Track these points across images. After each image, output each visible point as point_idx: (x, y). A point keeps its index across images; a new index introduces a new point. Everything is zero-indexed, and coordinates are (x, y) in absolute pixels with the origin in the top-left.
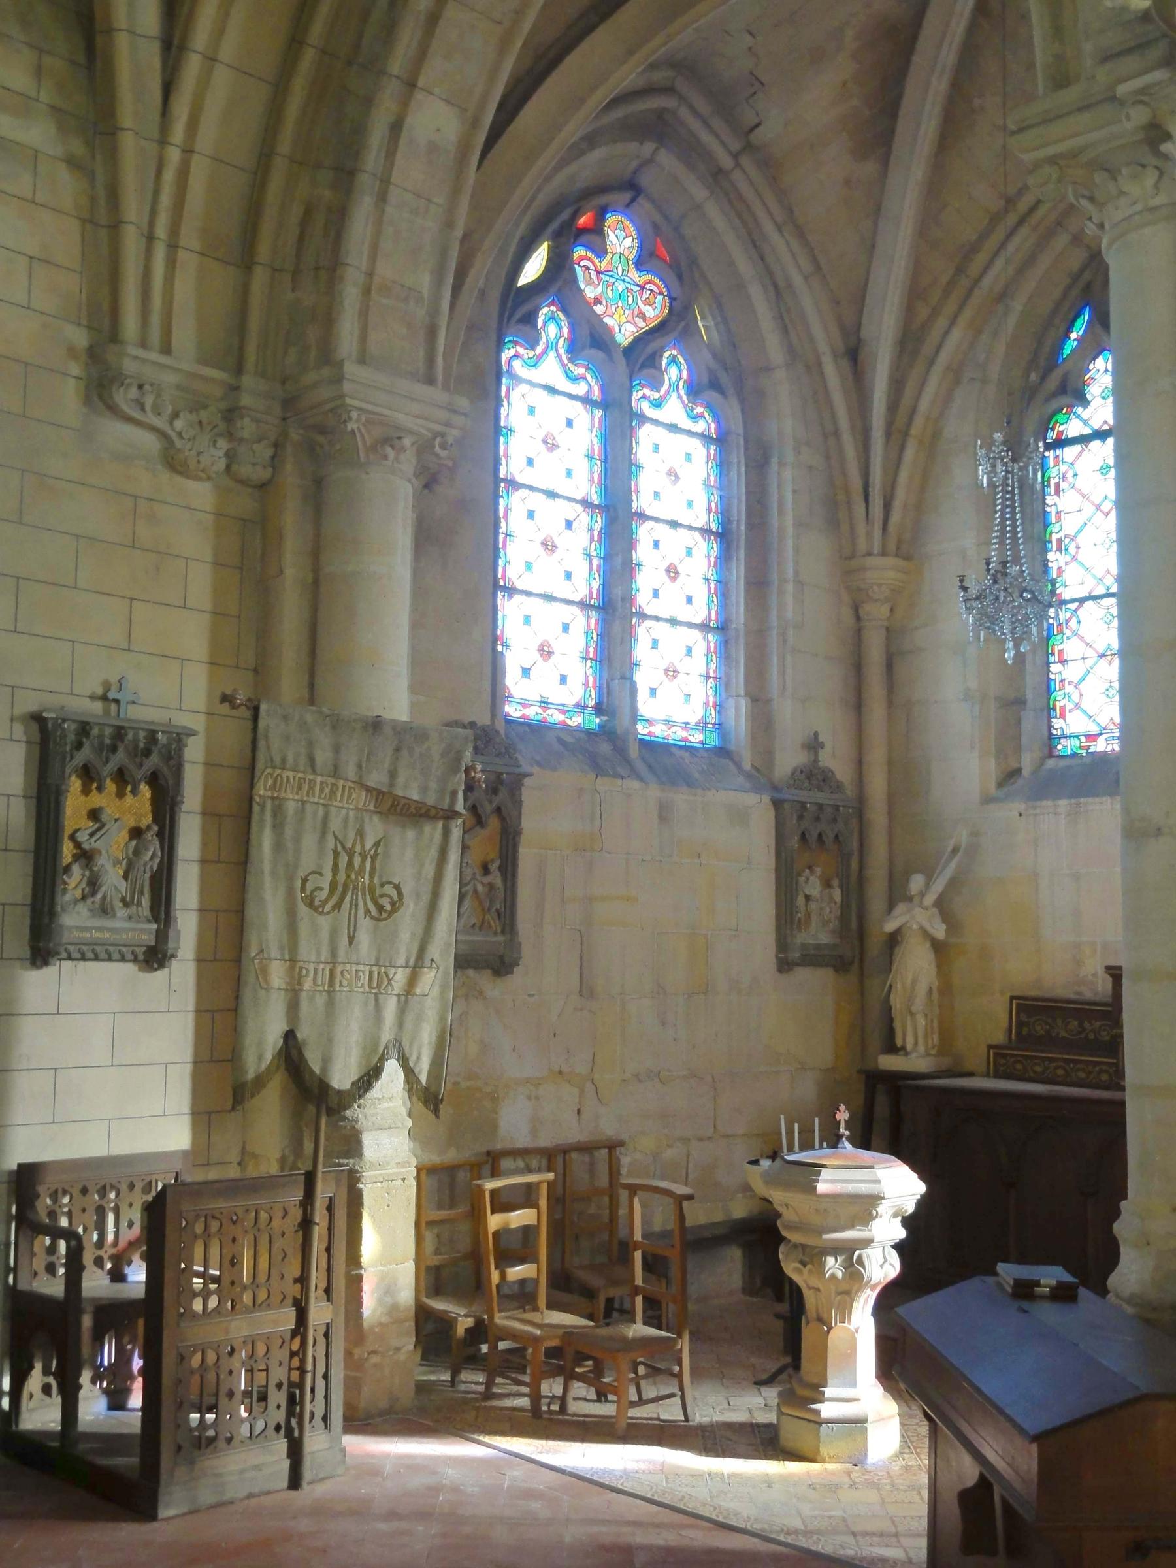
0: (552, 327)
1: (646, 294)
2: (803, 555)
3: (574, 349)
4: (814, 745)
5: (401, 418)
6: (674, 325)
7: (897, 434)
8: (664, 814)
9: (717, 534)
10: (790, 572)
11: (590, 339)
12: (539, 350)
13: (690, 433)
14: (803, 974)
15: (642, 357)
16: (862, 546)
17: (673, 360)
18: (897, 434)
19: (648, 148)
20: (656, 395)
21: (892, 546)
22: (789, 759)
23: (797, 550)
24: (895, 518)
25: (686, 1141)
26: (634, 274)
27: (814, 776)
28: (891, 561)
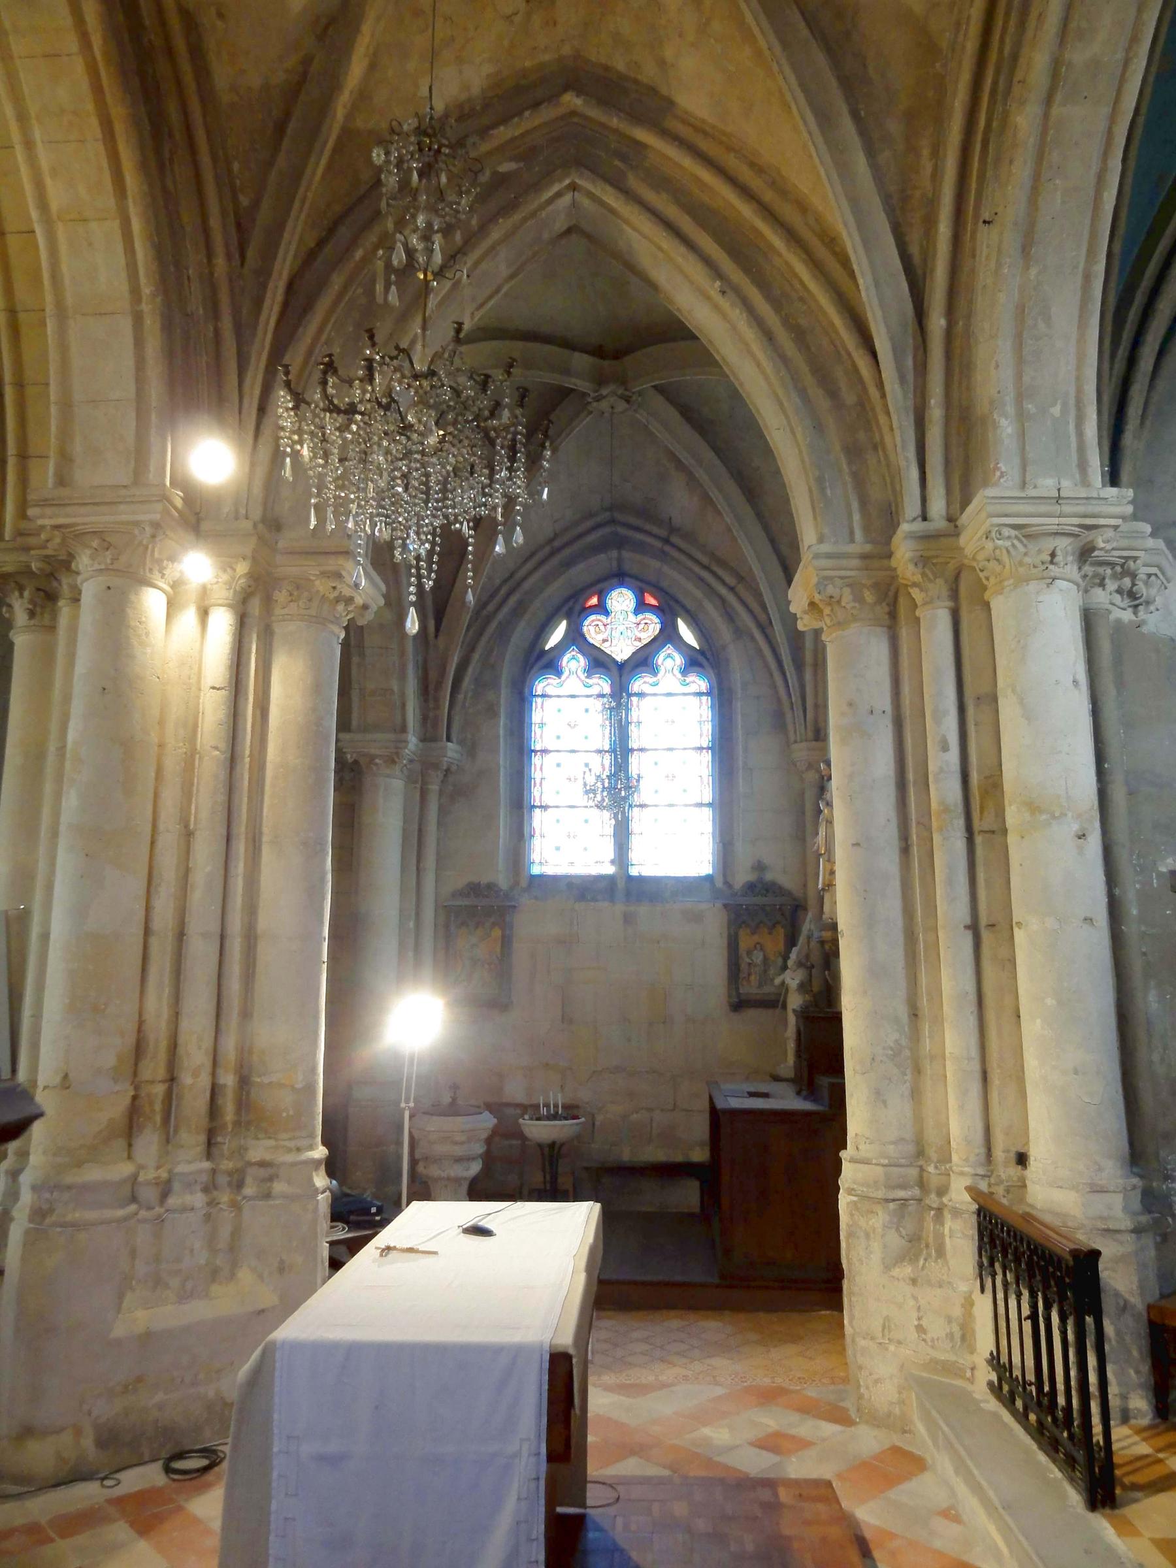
0: (574, 662)
1: (641, 626)
2: (760, 752)
3: (590, 672)
4: (760, 867)
5: (373, 751)
6: (668, 635)
7: (799, 666)
8: (628, 919)
9: (708, 748)
10: (740, 763)
11: (599, 662)
12: (563, 677)
13: (685, 694)
14: (752, 1013)
15: (643, 660)
16: (792, 739)
17: (669, 656)
18: (799, 666)
19: (614, 554)
20: (655, 679)
21: (810, 734)
22: (742, 877)
23: (746, 750)
24: (810, 715)
25: (650, 1110)
26: (632, 618)
27: (760, 887)
28: (804, 744)
